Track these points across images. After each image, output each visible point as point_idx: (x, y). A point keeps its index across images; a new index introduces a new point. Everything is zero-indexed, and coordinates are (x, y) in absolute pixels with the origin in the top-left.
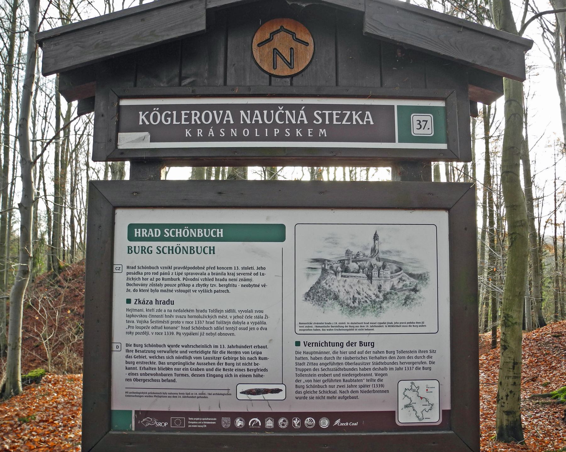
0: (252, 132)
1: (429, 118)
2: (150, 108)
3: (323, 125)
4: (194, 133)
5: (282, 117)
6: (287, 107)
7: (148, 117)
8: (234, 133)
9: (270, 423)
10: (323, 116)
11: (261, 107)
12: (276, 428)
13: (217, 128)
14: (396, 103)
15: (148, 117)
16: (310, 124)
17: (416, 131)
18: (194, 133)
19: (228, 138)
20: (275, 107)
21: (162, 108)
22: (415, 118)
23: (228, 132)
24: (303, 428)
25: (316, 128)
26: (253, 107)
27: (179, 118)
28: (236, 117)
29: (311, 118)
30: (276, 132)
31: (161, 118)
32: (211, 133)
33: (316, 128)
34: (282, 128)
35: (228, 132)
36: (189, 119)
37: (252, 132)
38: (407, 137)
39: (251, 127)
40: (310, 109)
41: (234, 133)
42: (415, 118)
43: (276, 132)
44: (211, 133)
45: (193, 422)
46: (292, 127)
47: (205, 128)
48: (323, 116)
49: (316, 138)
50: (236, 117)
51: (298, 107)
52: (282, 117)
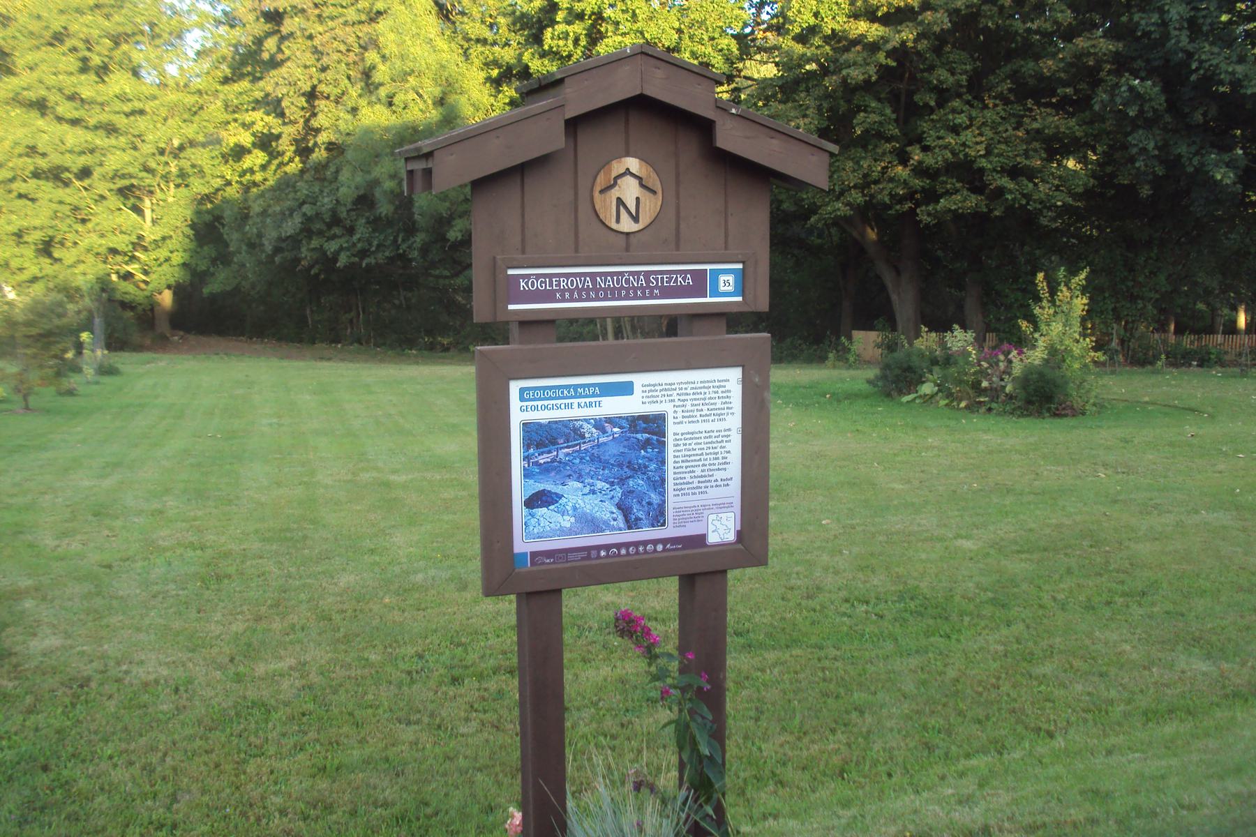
0: (606, 294)
1: (731, 278)
2: (528, 276)
3: (657, 287)
4: (563, 296)
5: (627, 281)
6: (631, 273)
7: (527, 284)
8: (593, 295)
9: (623, 552)
10: (657, 280)
11: (612, 274)
12: (628, 554)
13: (580, 291)
14: (708, 267)
15: (527, 284)
16: (648, 287)
17: (722, 288)
18: (563, 296)
19: (589, 299)
20: (622, 274)
21: (538, 276)
22: (722, 278)
23: (588, 294)
24: (646, 552)
25: (652, 289)
26: (606, 274)
27: (551, 285)
28: (594, 282)
29: (648, 281)
30: (623, 293)
31: (537, 284)
32: (576, 295)
33: (652, 289)
34: (627, 290)
35: (588, 294)
36: (559, 285)
37: (606, 294)
38: (716, 293)
39: (605, 290)
40: (647, 274)
41: (593, 295)
42: (722, 278)
43: (623, 293)
44: (576, 295)
45: (571, 556)
46: (635, 289)
47: (571, 292)
48: (657, 280)
49: (652, 297)
50: (594, 282)
51: (638, 273)
52: (627, 281)
